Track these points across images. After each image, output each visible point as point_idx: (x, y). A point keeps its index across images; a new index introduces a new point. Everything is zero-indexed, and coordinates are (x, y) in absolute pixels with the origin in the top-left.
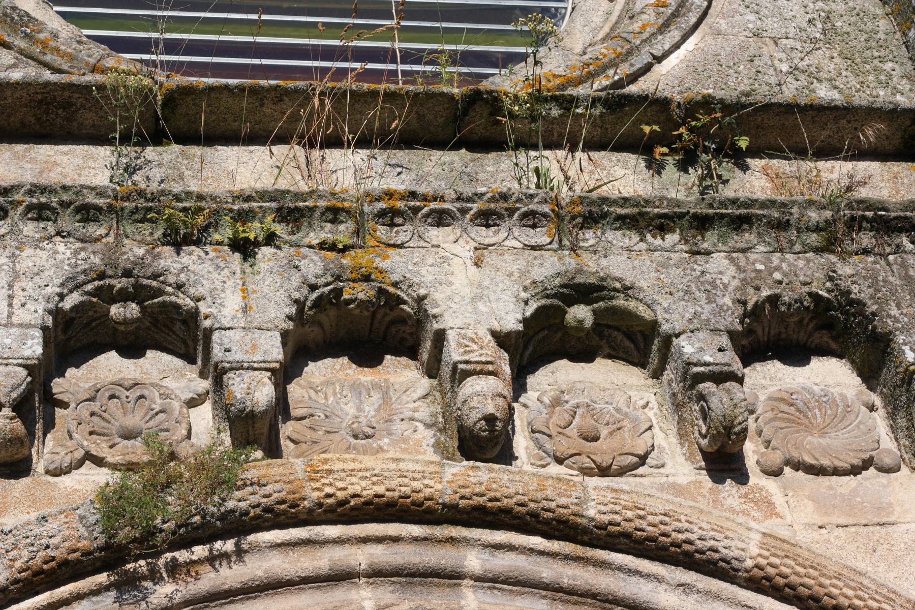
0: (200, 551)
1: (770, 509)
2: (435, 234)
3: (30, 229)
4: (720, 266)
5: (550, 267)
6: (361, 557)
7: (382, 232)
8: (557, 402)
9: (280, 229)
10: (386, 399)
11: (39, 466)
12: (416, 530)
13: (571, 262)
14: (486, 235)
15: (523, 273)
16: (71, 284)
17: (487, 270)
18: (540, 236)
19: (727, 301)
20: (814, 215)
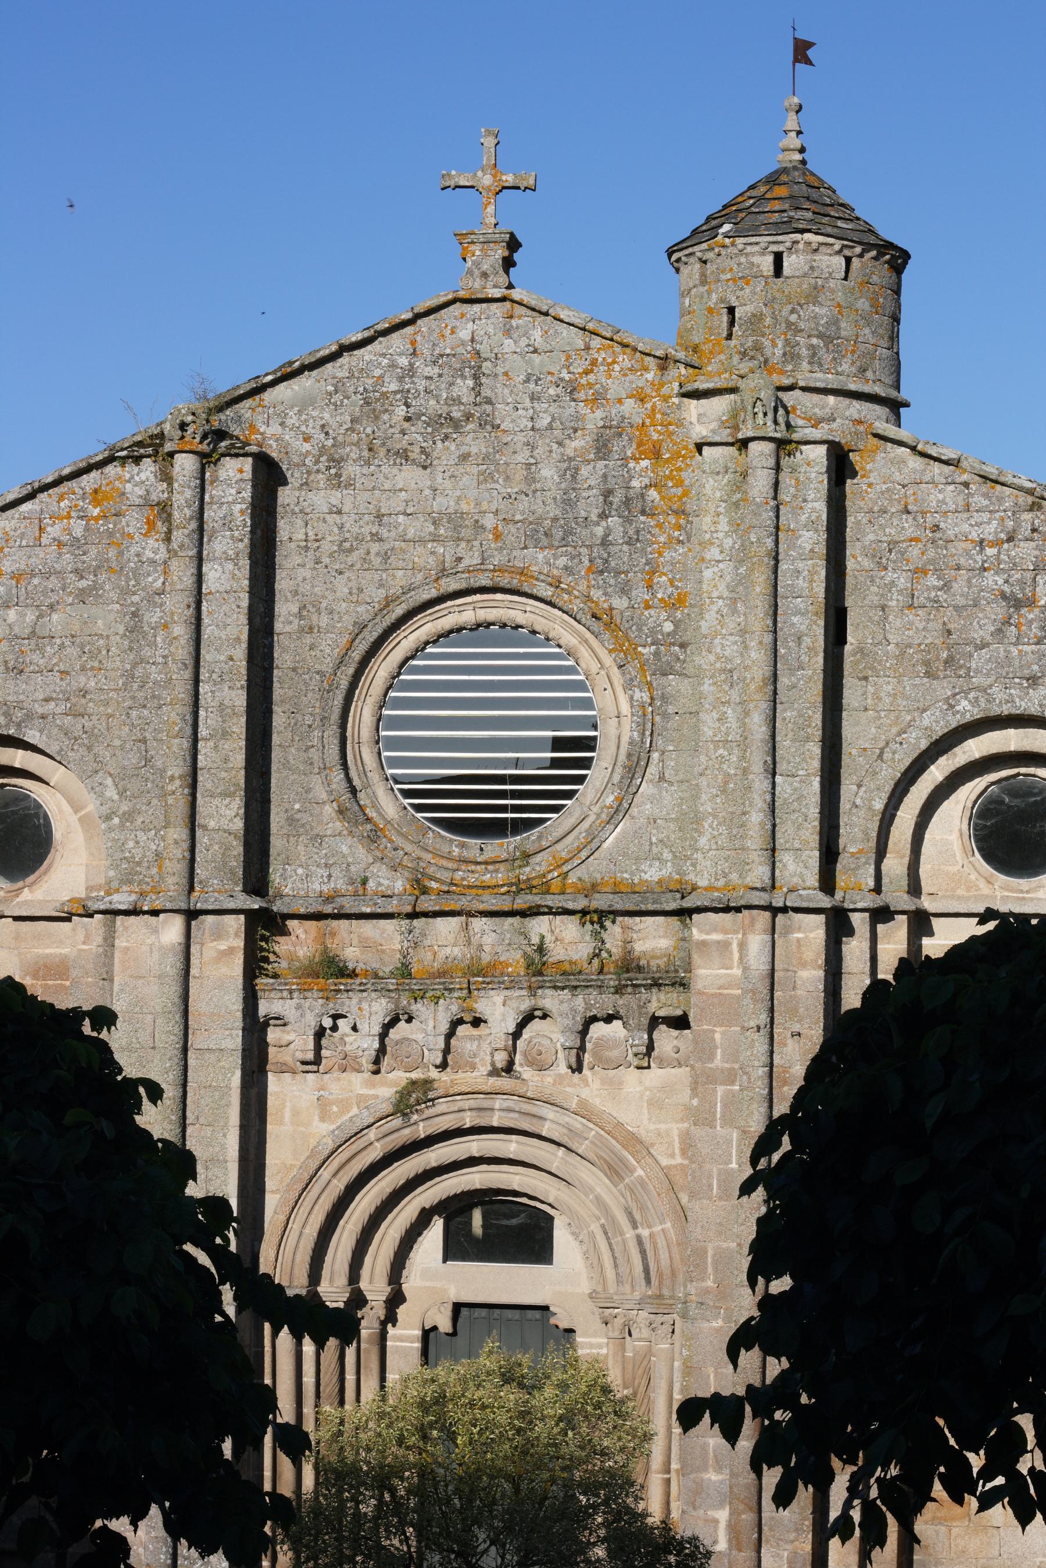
0: (423, 1106)
1: (587, 1084)
2: (492, 992)
3: (373, 995)
4: (579, 1002)
5: (526, 1005)
6: (466, 1105)
7: (476, 992)
8: (530, 1042)
9: (446, 993)
10: (479, 1044)
11: (383, 1070)
12: (482, 1096)
13: (533, 1002)
14: (507, 993)
15: (518, 1008)
16: (385, 1016)
17: (507, 1008)
18: (524, 992)
19: (578, 1019)
20: (612, 983)
